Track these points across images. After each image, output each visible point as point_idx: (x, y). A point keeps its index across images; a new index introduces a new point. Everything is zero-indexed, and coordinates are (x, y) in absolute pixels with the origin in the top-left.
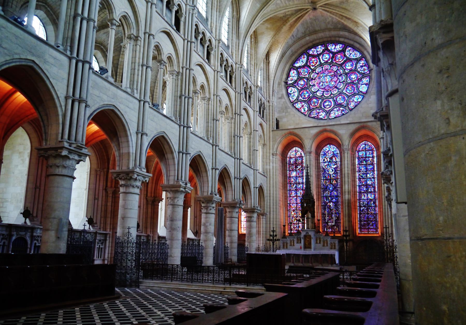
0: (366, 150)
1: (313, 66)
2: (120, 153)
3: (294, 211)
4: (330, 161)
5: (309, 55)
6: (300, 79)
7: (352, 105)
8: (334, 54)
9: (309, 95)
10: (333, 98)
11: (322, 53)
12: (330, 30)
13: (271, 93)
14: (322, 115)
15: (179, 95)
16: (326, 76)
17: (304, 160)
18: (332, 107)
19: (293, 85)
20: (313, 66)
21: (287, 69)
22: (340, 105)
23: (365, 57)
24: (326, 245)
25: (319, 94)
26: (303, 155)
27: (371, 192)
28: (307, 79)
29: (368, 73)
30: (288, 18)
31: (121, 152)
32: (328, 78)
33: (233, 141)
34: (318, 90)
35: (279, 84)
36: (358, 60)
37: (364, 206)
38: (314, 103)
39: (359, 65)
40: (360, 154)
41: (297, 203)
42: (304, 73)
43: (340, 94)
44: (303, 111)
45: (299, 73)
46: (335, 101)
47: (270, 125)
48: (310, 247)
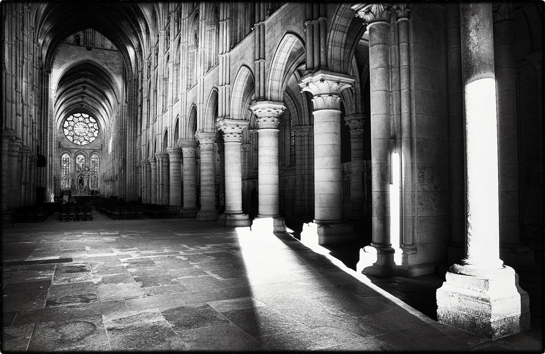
0: (95, 158)
5: (74, 116)
6: (69, 125)
8: (85, 118)
10: (83, 137)
17: (70, 160)
21: (64, 121)
23: (97, 122)
25: (78, 134)
26: (69, 158)
28: (73, 127)
29: (98, 129)
32: (82, 128)
35: (60, 127)
36: (95, 123)
40: (93, 160)
42: (72, 124)
44: (70, 140)
45: (69, 123)
46: (84, 138)
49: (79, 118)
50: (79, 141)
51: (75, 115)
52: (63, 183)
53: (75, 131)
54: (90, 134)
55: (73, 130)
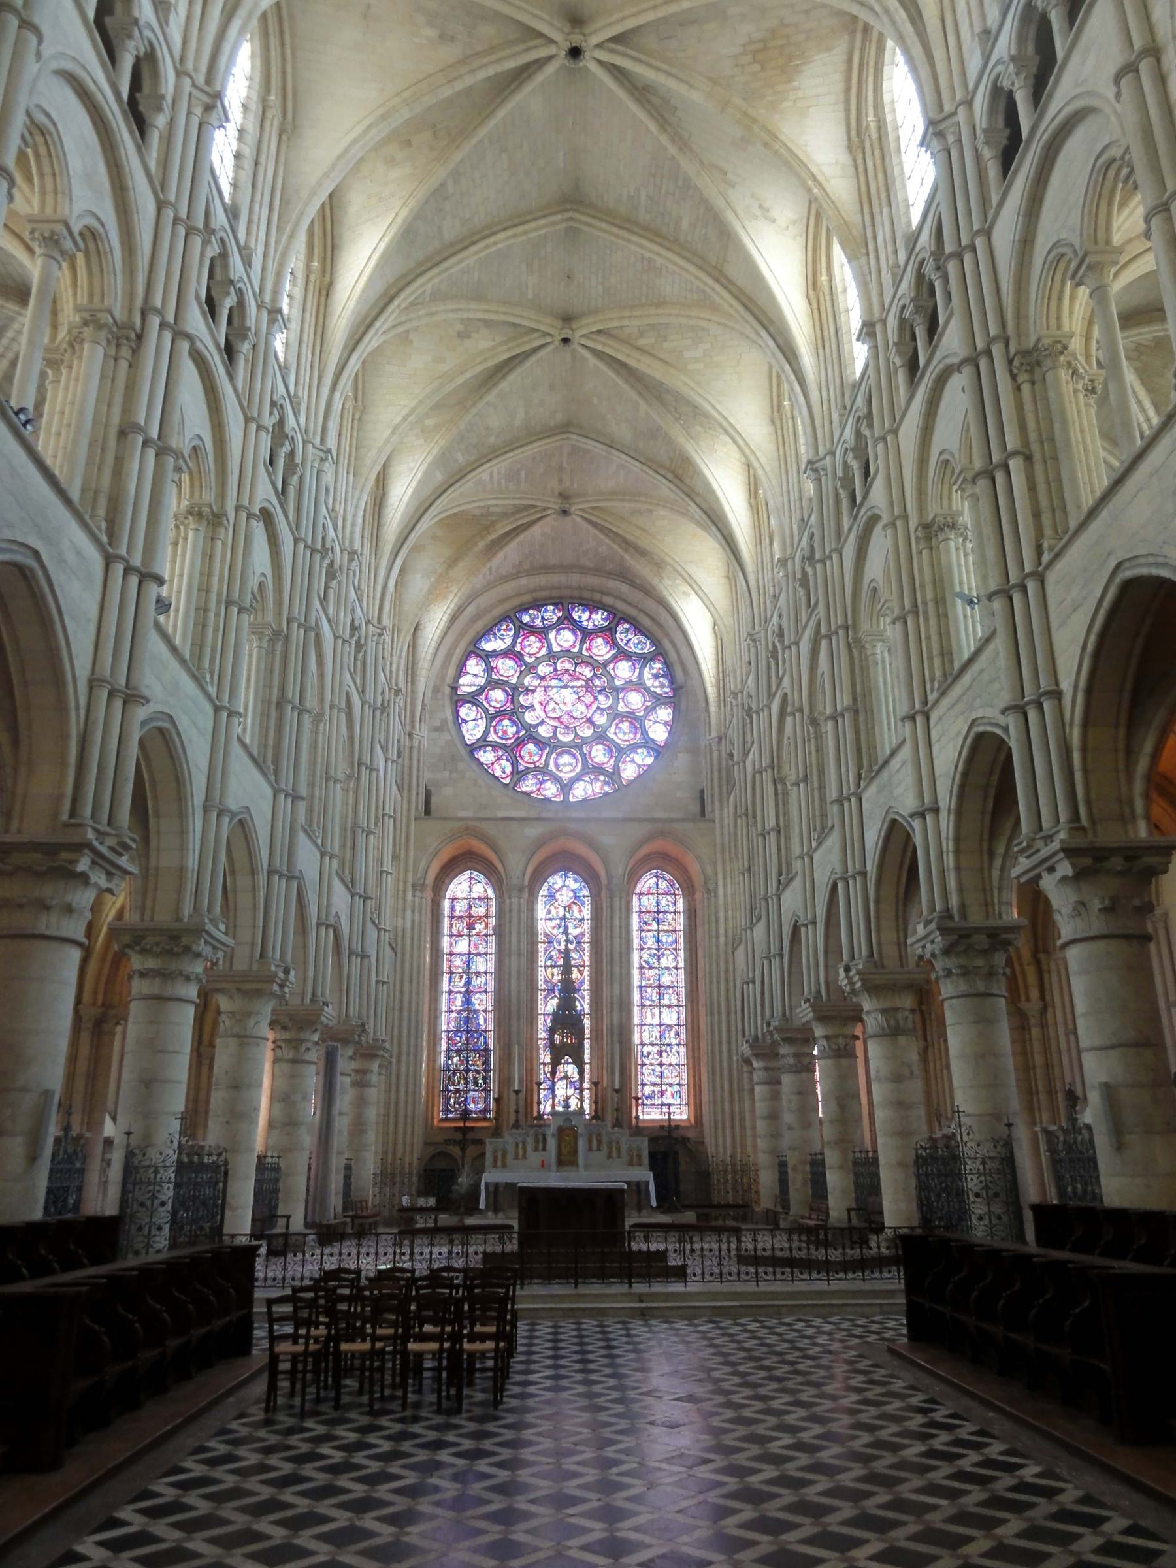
1: (530, 655)
2: (147, 869)
3: (458, 1052)
4: (564, 918)
7: (629, 772)
9: (518, 732)
10: (579, 747)
11: (558, 626)
12: (583, 570)
13: (418, 714)
14: (551, 790)
15: (274, 698)
16: (566, 687)
18: (578, 770)
19: (472, 699)
20: (530, 655)
21: (459, 652)
22: (599, 769)
24: (614, 1154)
25: (544, 732)
27: (669, 1006)
28: (514, 688)
30: (493, 523)
31: (153, 863)
33: (348, 844)
34: (542, 722)
35: (436, 690)
37: (652, 1044)
38: (530, 755)
39: (647, 674)
40: (644, 899)
41: (468, 1032)
42: (506, 668)
43: (600, 737)
44: (498, 773)
45: (489, 669)
47: (409, 802)
48: (573, 1163)
49: (552, 635)
50: (556, 779)
51: (526, 619)
52: (449, 1079)
53: (529, 717)
54: (625, 726)
55: (513, 712)
